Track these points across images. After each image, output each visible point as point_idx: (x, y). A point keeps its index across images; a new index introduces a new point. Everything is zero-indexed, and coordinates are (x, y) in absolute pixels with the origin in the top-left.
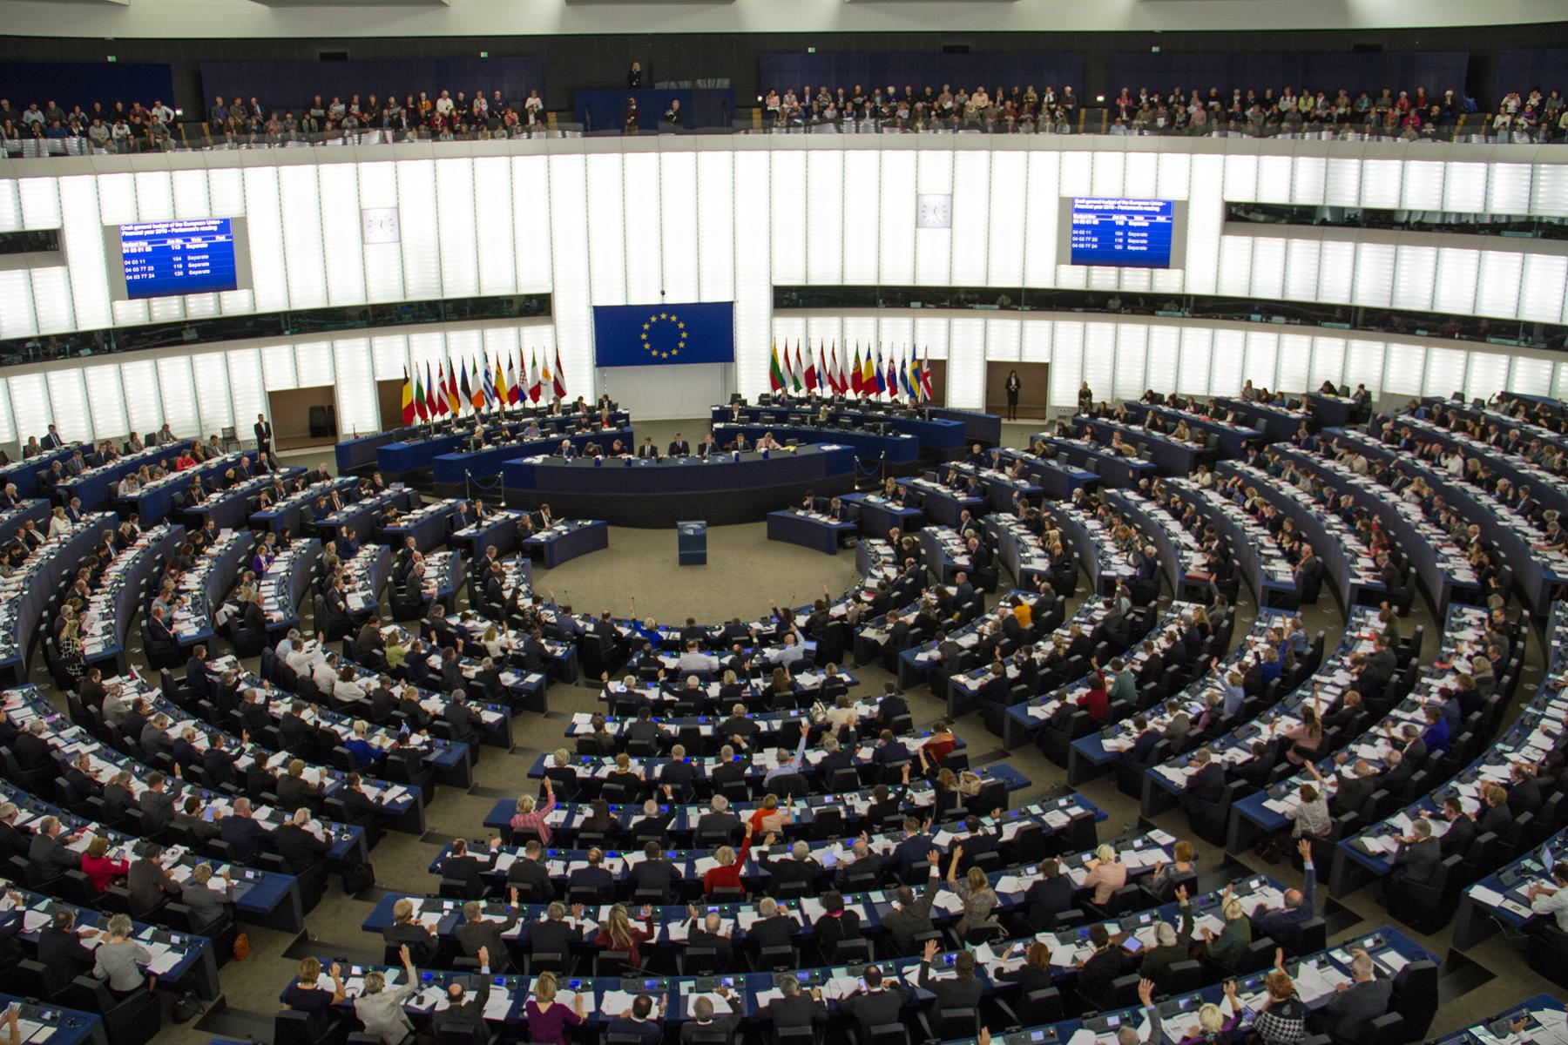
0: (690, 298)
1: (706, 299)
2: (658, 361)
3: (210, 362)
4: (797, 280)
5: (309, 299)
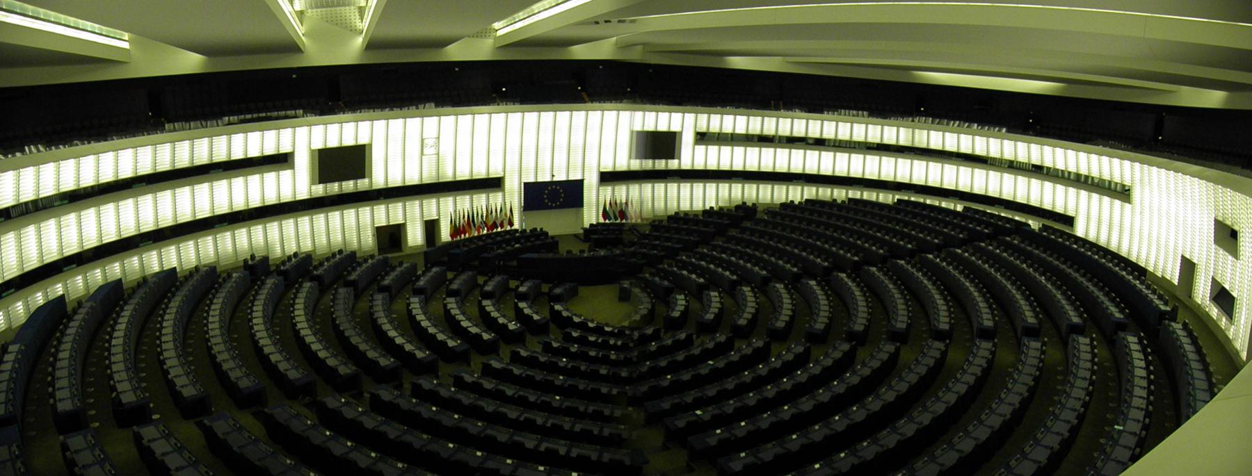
0: (563, 178)
1: (571, 178)
2: (551, 208)
3: (350, 213)
4: (610, 169)
5: (396, 181)
